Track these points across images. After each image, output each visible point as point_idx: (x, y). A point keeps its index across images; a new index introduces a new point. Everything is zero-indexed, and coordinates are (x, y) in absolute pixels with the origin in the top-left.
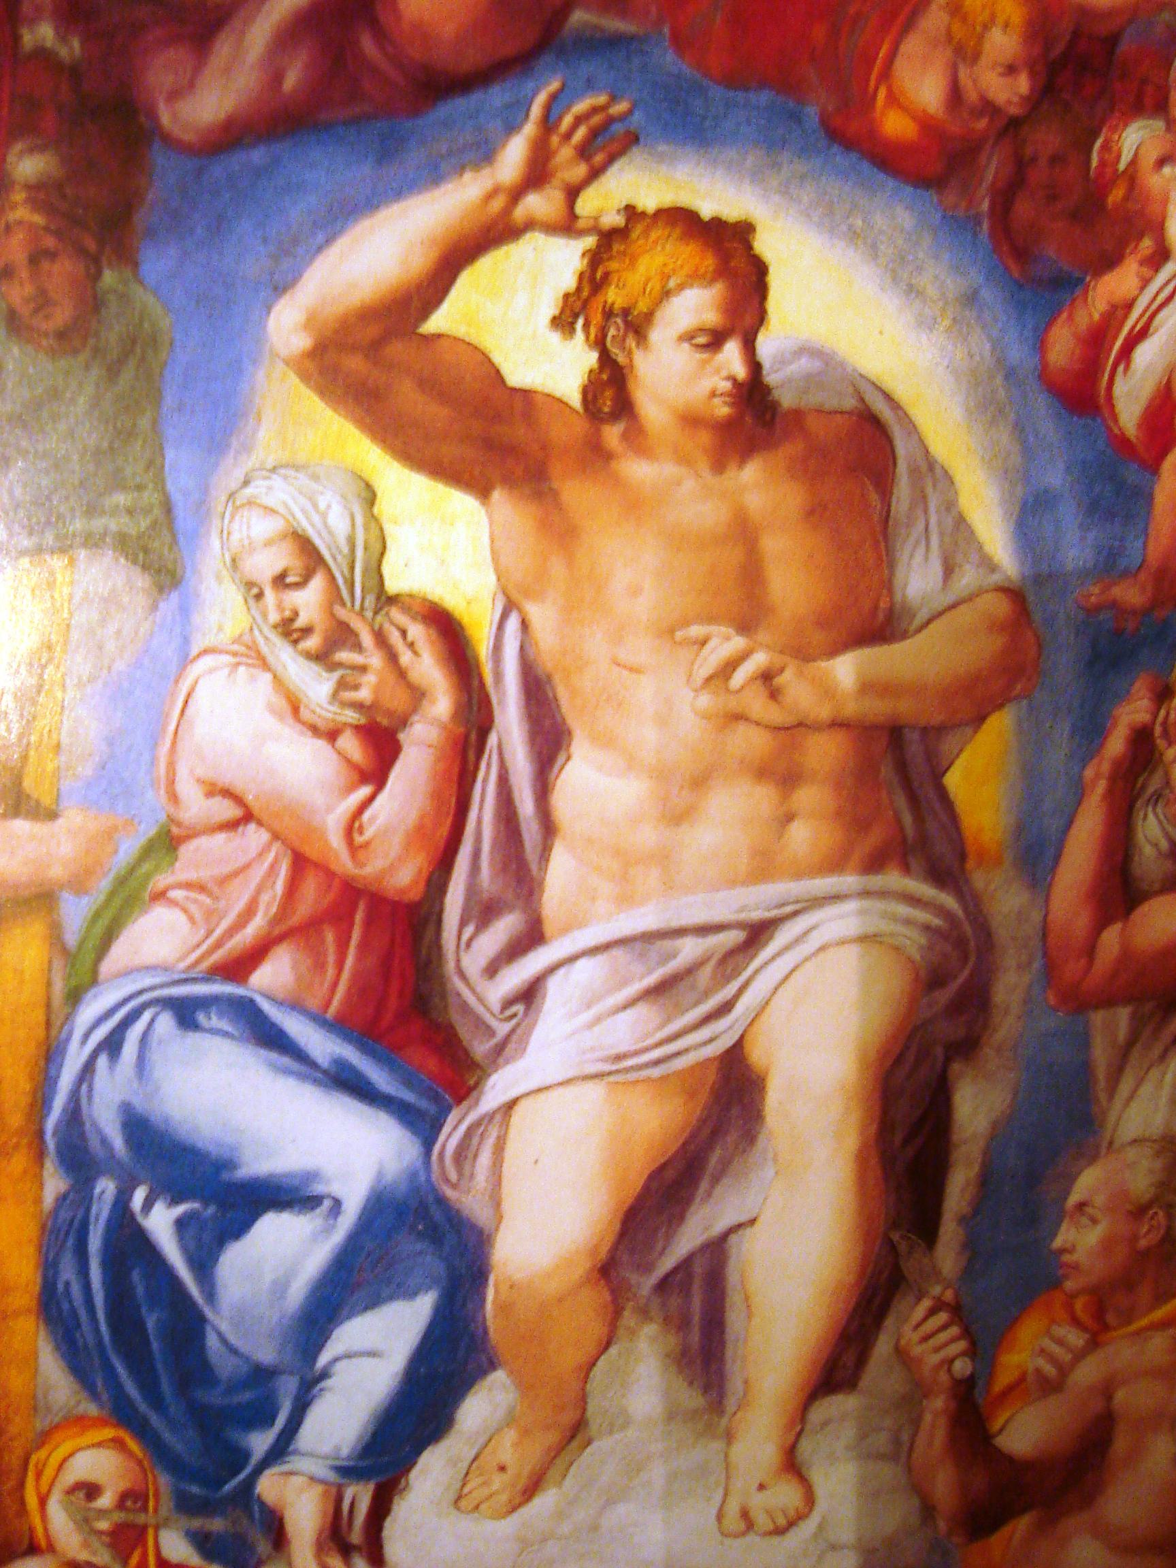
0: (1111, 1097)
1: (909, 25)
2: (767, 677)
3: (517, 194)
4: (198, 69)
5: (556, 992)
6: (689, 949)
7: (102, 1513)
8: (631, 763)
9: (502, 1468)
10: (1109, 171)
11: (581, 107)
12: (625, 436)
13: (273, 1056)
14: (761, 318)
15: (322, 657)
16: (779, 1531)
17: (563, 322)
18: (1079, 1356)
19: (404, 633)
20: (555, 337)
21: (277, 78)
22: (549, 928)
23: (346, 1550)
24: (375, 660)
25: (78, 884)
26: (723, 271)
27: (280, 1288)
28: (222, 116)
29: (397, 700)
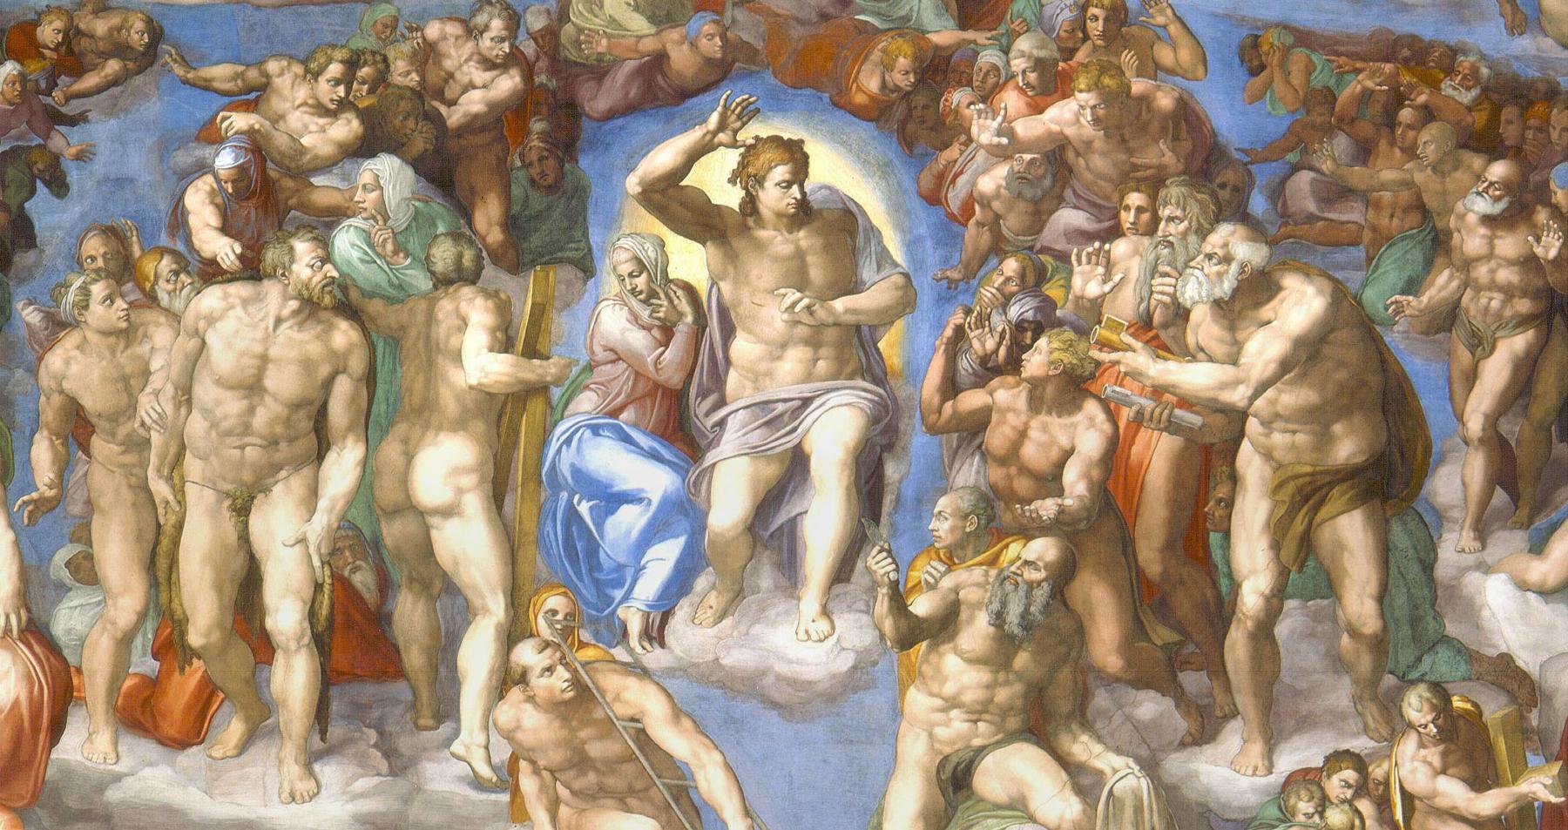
0: (951, 469)
1: (866, 58)
2: (808, 307)
3: (715, 133)
4: (598, 91)
5: (732, 423)
6: (780, 407)
7: (558, 622)
8: (760, 340)
9: (711, 607)
10: (948, 110)
11: (738, 100)
12: (755, 221)
13: (627, 445)
14: (806, 175)
15: (646, 302)
16: (821, 641)
17: (732, 181)
18: (942, 576)
19: (675, 293)
20: (730, 185)
21: (627, 94)
22: (728, 400)
23: (650, 639)
24: (666, 303)
25: (558, 383)
26: (792, 159)
27: (628, 533)
28: (608, 107)
29: (674, 318)
